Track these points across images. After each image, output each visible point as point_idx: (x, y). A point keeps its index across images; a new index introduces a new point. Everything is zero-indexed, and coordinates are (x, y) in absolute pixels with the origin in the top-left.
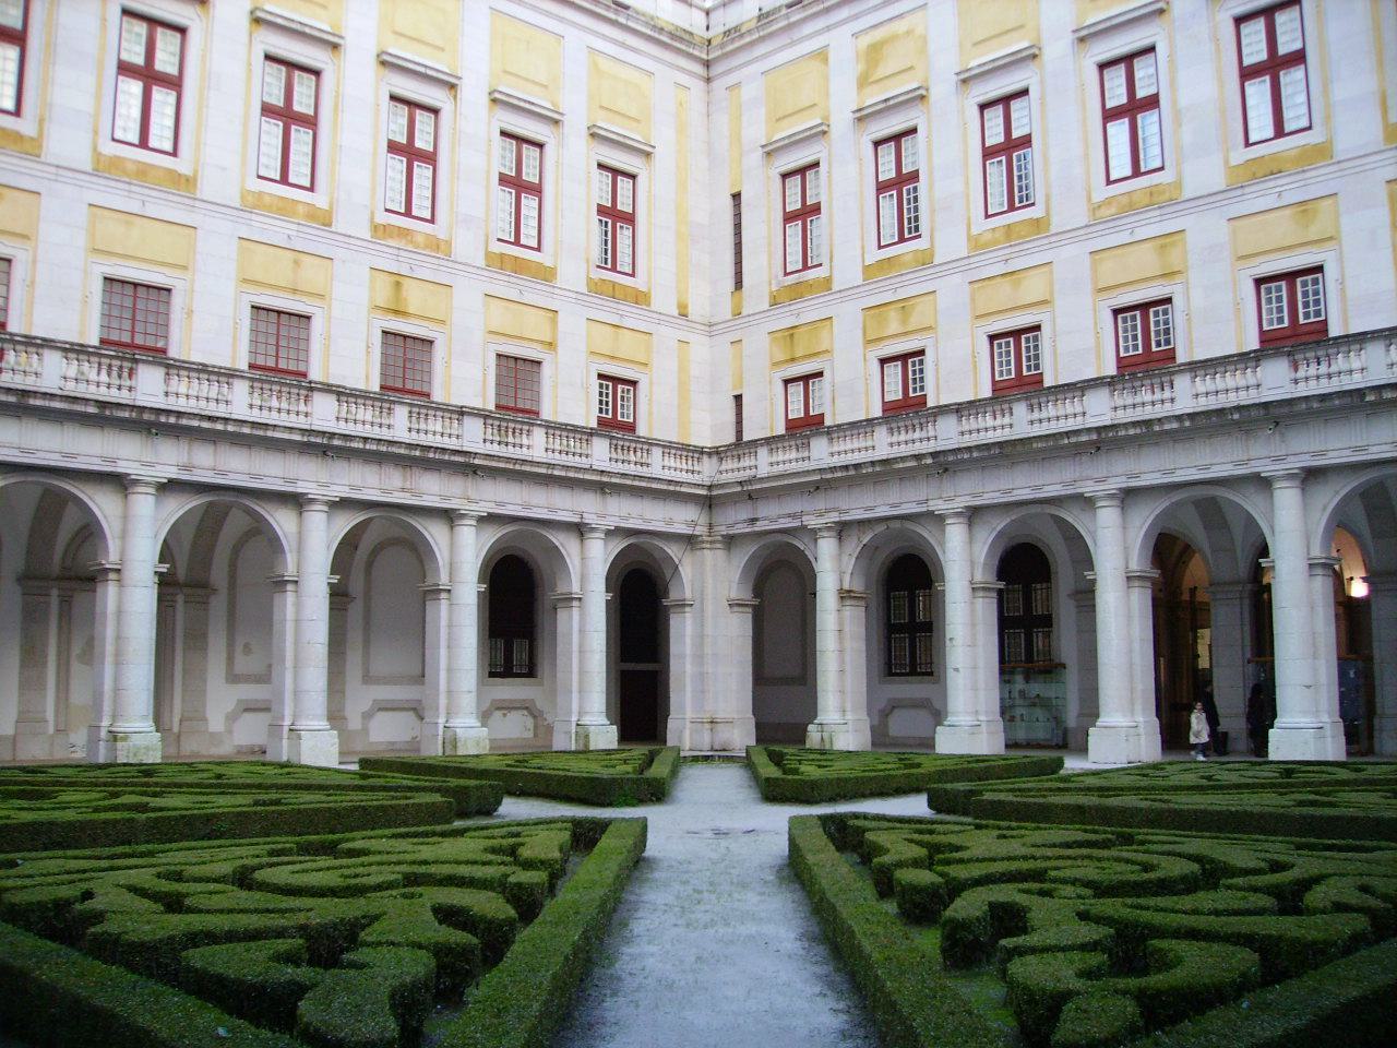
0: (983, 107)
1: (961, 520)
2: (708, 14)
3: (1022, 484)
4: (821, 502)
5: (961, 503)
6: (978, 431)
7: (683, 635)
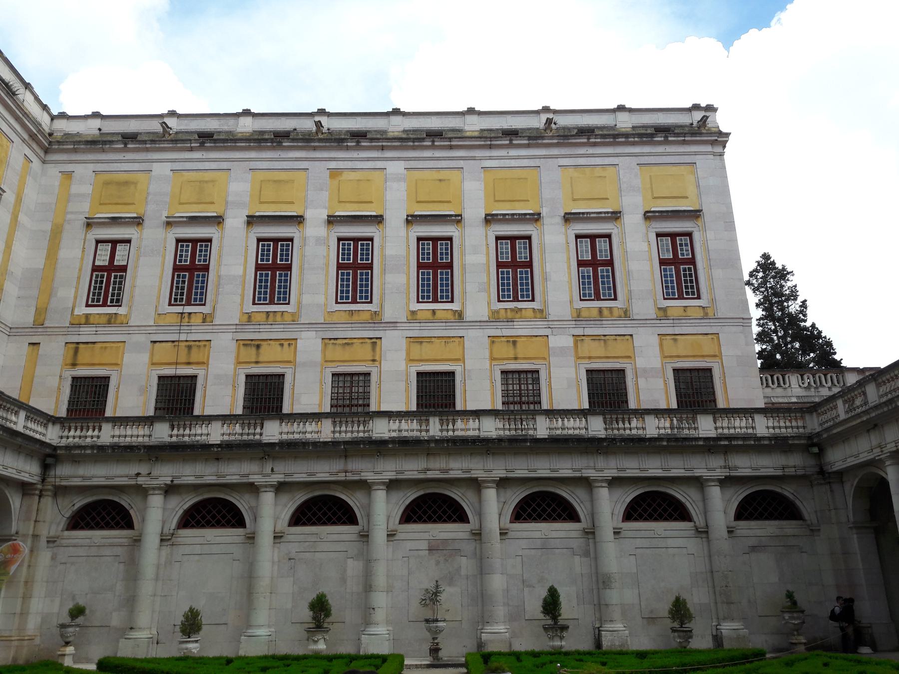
1: (272, 489)
2: (52, 119)
4: (601, 462)
5: (277, 478)
6: (126, 436)
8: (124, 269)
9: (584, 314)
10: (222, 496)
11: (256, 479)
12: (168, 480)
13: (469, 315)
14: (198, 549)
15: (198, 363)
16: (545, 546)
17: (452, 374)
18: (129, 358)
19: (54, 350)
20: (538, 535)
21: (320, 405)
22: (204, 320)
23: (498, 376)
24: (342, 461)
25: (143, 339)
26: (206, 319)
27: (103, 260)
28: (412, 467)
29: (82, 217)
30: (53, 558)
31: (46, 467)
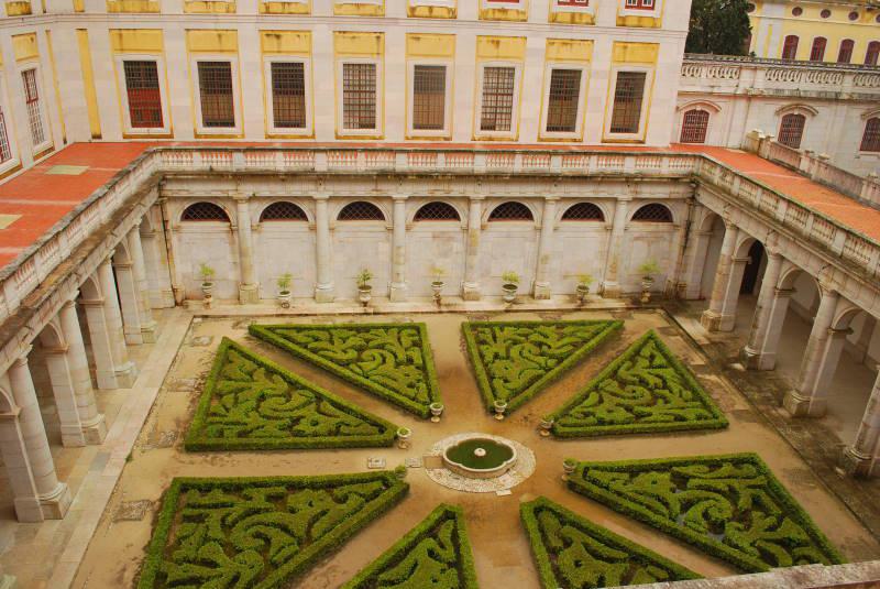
9: (559, 18)
12: (251, 194)
13: (461, 15)
15: (229, 51)
16: (508, 236)
17: (444, 68)
18: (169, 45)
20: (505, 230)
23: (482, 71)
28: (425, 190)
30: (180, 240)
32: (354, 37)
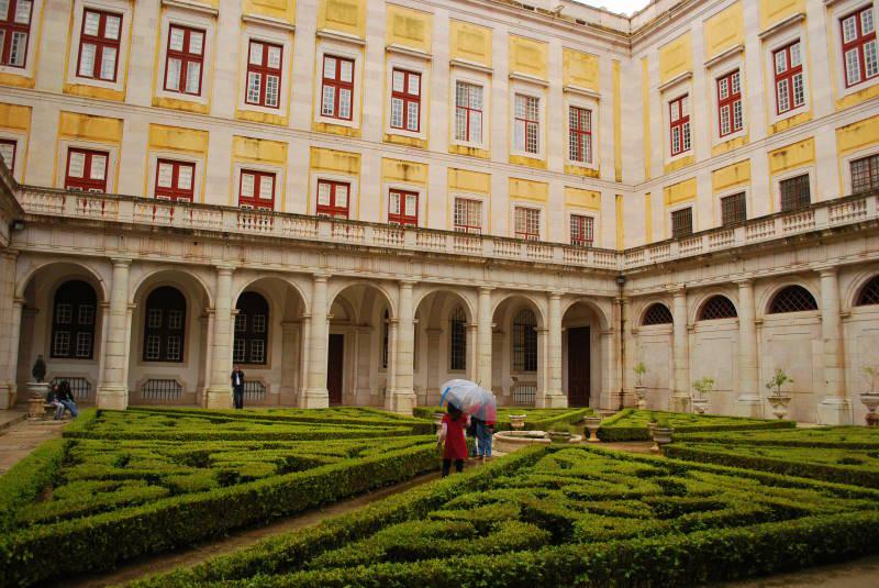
0: (775, 52)
3: (780, 265)
5: (748, 275)
7: (472, 338)
8: (687, 119)
10: (719, 293)
11: (734, 278)
12: (681, 286)
14: (710, 335)
15: (744, 181)
19: (658, 193)
21: (841, 192)
22: (743, 143)
24: (793, 255)
25: (706, 172)
26: (745, 142)
27: (676, 118)
29: (655, 89)
30: (637, 344)
31: (621, 285)
32: (858, 128)
